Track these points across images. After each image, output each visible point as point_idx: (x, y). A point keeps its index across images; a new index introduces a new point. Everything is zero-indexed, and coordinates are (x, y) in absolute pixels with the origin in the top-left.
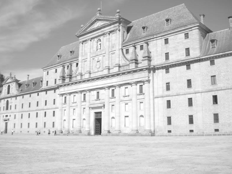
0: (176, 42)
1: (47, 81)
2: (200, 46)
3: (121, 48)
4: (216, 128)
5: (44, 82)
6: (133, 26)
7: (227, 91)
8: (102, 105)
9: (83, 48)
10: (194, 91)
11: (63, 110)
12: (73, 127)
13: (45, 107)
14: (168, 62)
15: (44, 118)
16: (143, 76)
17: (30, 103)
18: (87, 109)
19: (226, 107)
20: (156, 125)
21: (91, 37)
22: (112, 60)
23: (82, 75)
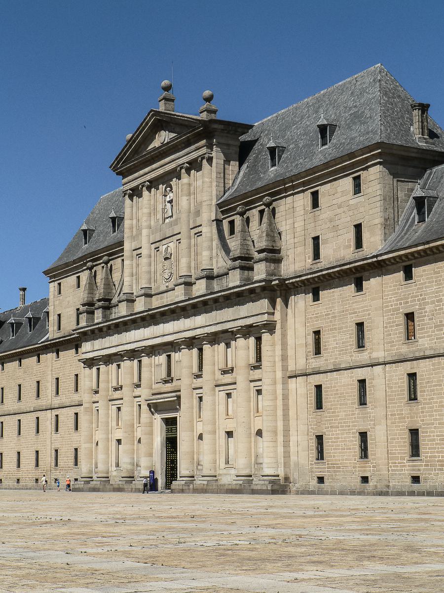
0: (334, 202)
1: (59, 315)
2: (386, 220)
3: (214, 218)
4: (415, 474)
5: (53, 318)
6: (258, 139)
7: (436, 360)
8: (171, 397)
9: (134, 211)
10: (370, 357)
11: (95, 412)
12: (117, 465)
13: (56, 402)
14: (320, 266)
15: (54, 436)
16: (252, 312)
17: (20, 386)
18: (145, 407)
19: (436, 411)
20: (293, 458)
21: (148, 177)
22: (197, 254)
23: (131, 301)
